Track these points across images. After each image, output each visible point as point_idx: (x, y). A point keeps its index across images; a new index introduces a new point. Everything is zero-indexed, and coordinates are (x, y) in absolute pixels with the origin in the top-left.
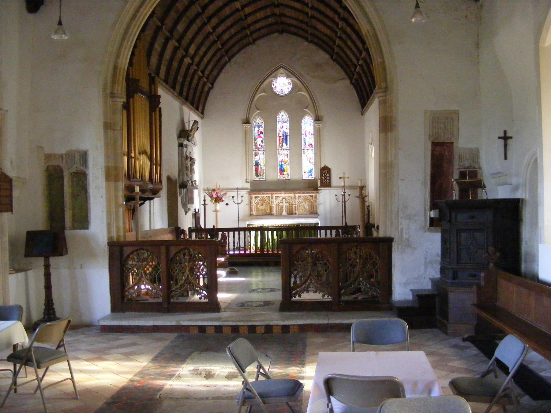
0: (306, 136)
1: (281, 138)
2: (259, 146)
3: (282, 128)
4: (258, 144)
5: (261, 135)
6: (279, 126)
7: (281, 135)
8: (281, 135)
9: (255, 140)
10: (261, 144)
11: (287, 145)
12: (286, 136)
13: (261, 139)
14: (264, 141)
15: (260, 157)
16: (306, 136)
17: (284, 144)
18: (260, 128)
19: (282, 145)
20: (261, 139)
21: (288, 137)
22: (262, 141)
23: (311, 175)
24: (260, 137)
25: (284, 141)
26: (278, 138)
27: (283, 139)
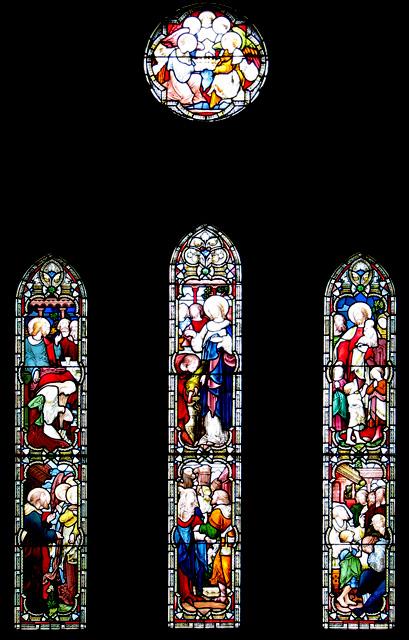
0: (349, 375)
3: (197, 327)
6: (182, 311)
8: (193, 365)
9: (31, 394)
11: (226, 425)
12: (226, 374)
13: (69, 387)
17: (213, 425)
18: (64, 323)
23: (374, 606)
24: (65, 376)
25: (212, 402)
27: (203, 389)
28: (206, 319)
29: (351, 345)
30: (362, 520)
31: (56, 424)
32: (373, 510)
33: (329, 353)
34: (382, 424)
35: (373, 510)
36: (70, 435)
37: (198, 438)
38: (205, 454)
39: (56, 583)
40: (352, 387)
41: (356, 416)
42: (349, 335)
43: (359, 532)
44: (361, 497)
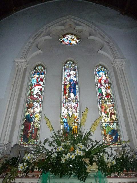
0: (101, 85)
1: (67, 87)
2: (35, 96)
3: (68, 76)
4: (35, 92)
5: (41, 83)
7: (68, 83)
8: (68, 83)
9: (32, 88)
10: (40, 93)
11: (75, 95)
12: (75, 85)
13: (40, 87)
14: (43, 89)
15: (35, 110)
16: (101, 85)
17: (72, 95)
18: (41, 75)
19: (69, 96)
20: (40, 87)
21: (77, 86)
22: (41, 90)
25: (72, 90)
26: (63, 86)
27: (70, 88)
28: (70, 75)
29: (101, 80)
30: (109, 117)
31: (37, 95)
32: (111, 114)
33: (97, 81)
34: (110, 95)
35: (111, 114)
36: (40, 97)
37: (69, 98)
38: (70, 101)
39: (31, 133)
40: (102, 87)
41: (104, 93)
42: (100, 78)
43: (109, 119)
44: (108, 111)
